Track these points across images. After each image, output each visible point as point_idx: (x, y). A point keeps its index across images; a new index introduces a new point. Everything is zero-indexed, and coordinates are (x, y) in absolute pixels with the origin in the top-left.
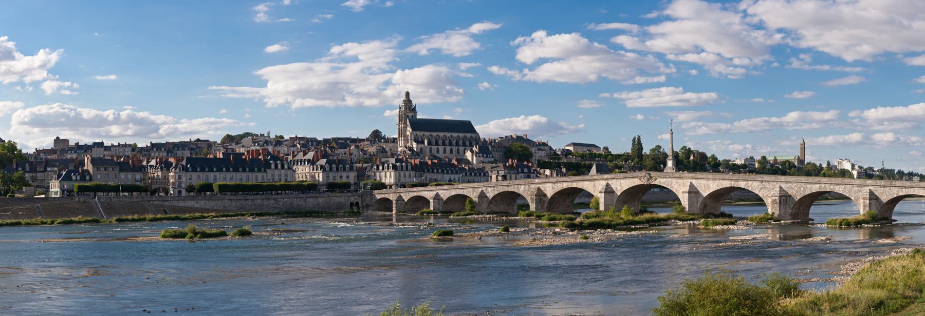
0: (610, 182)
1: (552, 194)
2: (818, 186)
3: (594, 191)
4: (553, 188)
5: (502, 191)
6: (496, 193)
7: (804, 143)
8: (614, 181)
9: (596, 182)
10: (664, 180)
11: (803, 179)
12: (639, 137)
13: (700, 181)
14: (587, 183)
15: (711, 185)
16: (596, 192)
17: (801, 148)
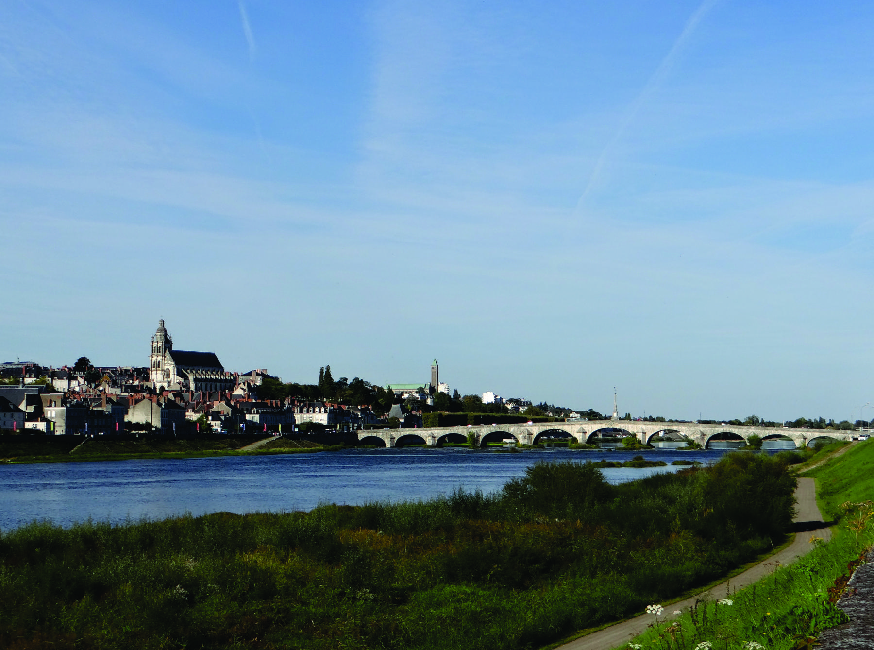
0: (583, 426)
1: (538, 434)
2: (722, 429)
3: (571, 432)
4: (538, 429)
5: (494, 431)
6: (489, 432)
7: (437, 366)
8: (587, 426)
9: (573, 426)
10: (623, 425)
11: (540, 424)
12: (328, 368)
13: (647, 426)
14: (566, 426)
15: (655, 429)
16: (573, 432)
17: (433, 372)
